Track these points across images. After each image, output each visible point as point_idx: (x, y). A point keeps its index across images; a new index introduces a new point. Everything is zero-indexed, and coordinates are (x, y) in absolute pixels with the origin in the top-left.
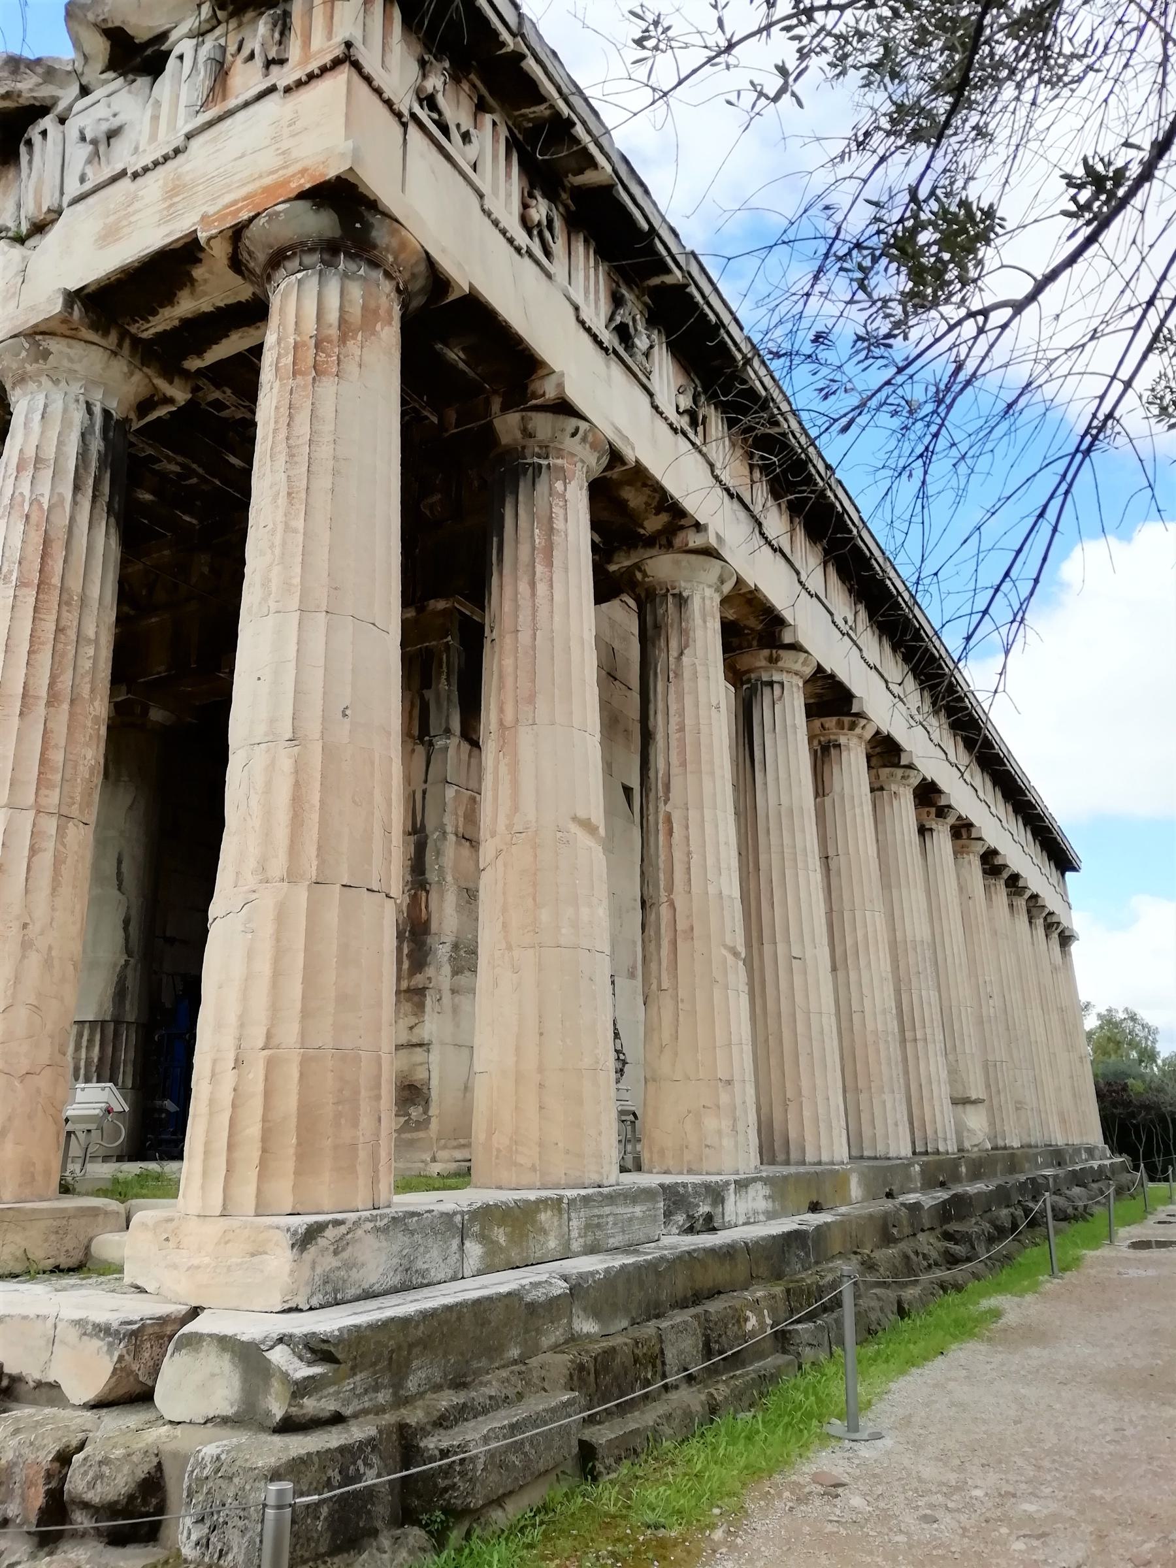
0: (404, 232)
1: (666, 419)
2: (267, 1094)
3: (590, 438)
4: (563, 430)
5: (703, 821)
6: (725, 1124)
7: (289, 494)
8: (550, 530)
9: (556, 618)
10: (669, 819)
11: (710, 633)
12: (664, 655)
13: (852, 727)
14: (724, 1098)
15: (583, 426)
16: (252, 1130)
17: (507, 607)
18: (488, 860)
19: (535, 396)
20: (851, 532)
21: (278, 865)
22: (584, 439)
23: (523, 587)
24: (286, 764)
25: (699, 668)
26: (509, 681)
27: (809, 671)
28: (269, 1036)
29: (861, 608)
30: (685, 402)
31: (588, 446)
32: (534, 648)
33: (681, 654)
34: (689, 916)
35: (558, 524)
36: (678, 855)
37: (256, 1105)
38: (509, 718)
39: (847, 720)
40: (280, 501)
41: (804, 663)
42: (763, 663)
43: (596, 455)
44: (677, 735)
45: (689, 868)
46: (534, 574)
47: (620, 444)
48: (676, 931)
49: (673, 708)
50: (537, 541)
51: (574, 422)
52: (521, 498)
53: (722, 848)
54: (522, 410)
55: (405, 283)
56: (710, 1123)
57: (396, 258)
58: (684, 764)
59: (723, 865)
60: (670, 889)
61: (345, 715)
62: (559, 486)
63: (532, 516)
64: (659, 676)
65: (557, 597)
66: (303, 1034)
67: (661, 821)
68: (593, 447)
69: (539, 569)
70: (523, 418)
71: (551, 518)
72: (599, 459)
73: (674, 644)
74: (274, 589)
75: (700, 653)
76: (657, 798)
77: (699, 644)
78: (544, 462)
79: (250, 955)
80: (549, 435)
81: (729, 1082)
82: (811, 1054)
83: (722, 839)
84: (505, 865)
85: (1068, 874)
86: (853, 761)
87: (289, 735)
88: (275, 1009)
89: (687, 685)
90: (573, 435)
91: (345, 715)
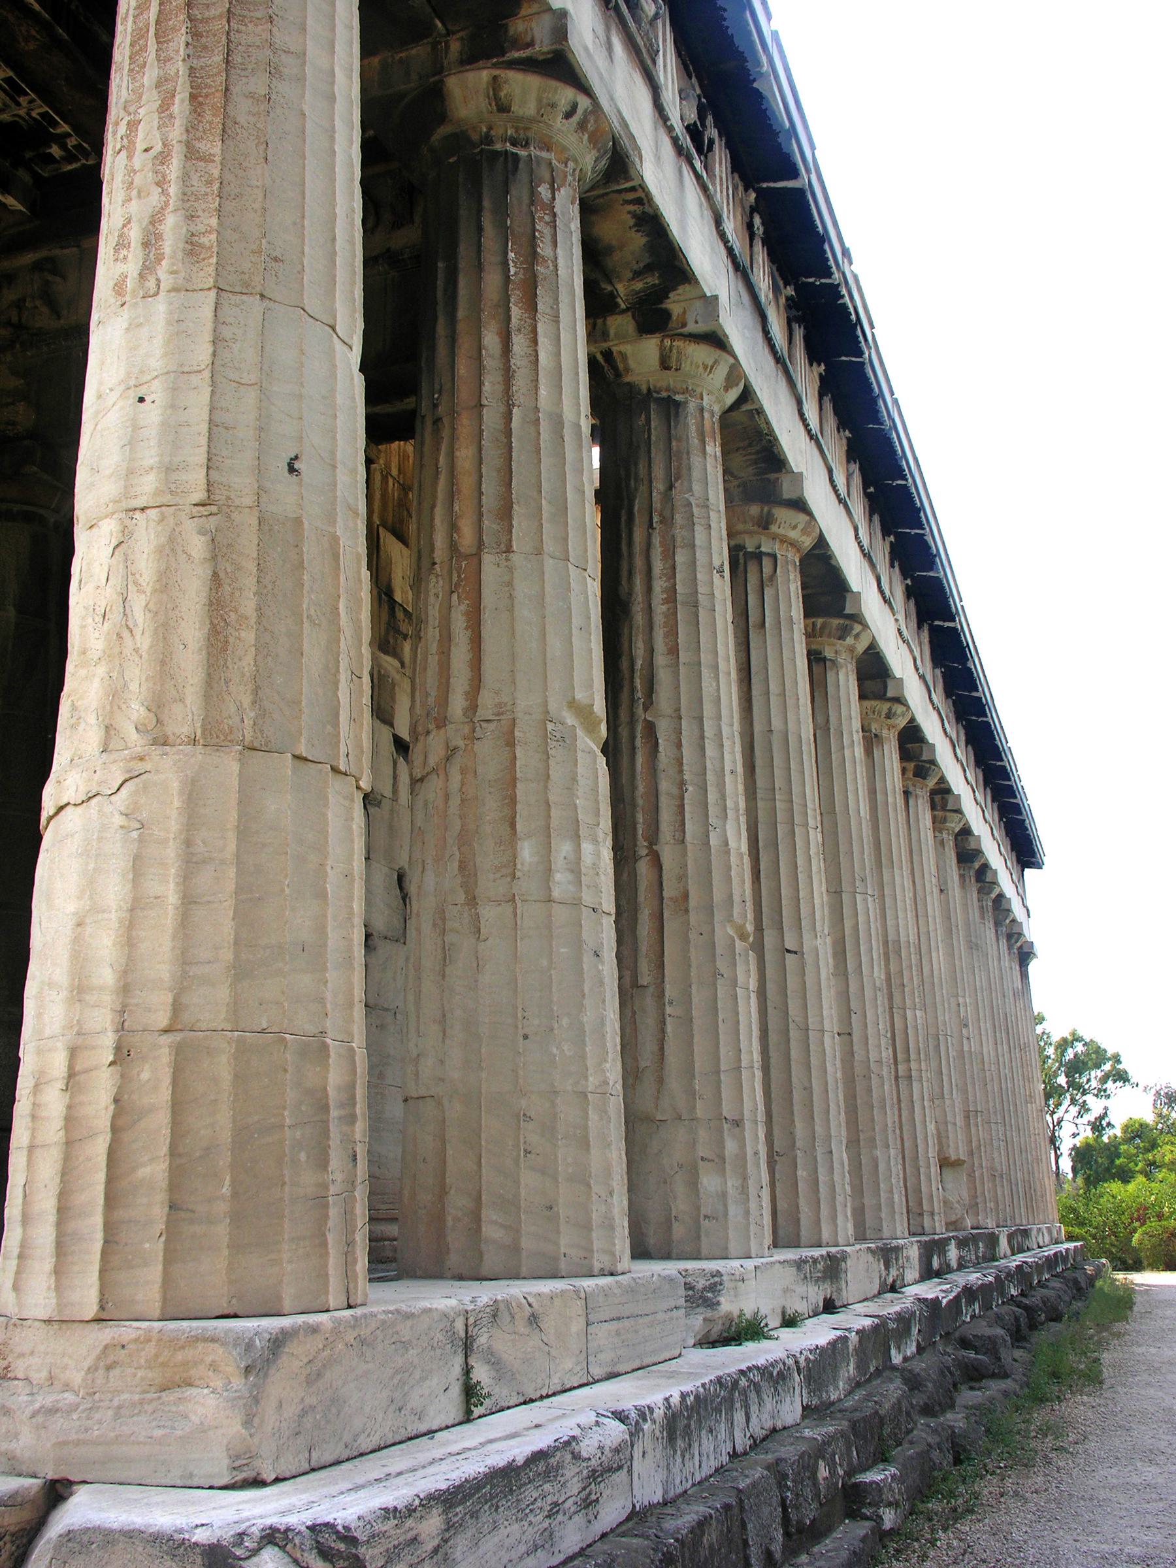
1: (670, 129)
2: (177, 1107)
3: (591, 126)
5: (702, 737)
6: (732, 1183)
7: (193, 97)
8: (533, 256)
9: (543, 392)
10: (651, 728)
11: (710, 462)
12: (643, 488)
13: (843, 633)
14: (731, 1147)
15: (584, 102)
16: (152, 1170)
17: (463, 369)
18: (432, 761)
19: (517, 44)
20: (861, 354)
21: (186, 717)
23: (491, 340)
24: (197, 546)
25: (696, 510)
26: (466, 483)
27: (808, 542)
28: (177, 1008)
29: (855, 467)
30: (692, 116)
32: (508, 433)
33: (671, 487)
34: (682, 877)
35: (544, 249)
36: (665, 786)
37: (158, 1123)
38: (467, 539)
39: (836, 622)
40: (176, 109)
41: (804, 532)
42: (749, 527)
43: (594, 154)
44: (664, 608)
45: (682, 806)
46: (509, 318)
47: (625, 142)
48: (662, 899)
49: (658, 566)
50: (512, 271)
52: (486, 204)
53: (728, 778)
54: (495, 66)
56: (709, 1182)
58: (674, 651)
59: (729, 803)
60: (653, 838)
61: (292, 469)
62: (544, 191)
63: (504, 233)
64: (637, 521)
66: (236, 1006)
67: (639, 735)
68: (594, 139)
69: (516, 312)
70: (495, 78)
73: (658, 472)
74: (167, 249)
75: (697, 487)
76: (633, 701)
77: (696, 474)
78: (523, 153)
79: (138, 868)
81: (738, 1123)
82: (808, 1089)
83: (728, 767)
84: (463, 771)
85: (1027, 871)
86: (846, 682)
87: (199, 495)
88: (184, 959)
89: (679, 533)
90: (568, 115)
91: (292, 469)
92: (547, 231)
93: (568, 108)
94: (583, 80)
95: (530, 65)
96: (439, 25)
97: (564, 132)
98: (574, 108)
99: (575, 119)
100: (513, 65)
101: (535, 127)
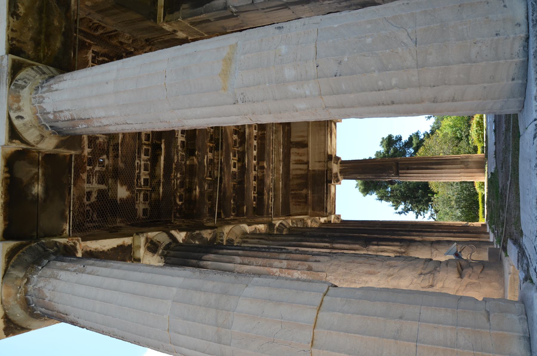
0: (4, 298)
3: (15, 106)
4: (25, 125)
15: (13, 115)
22: (19, 109)
31: (21, 104)
50: (85, 126)
51: (16, 122)
54: (34, 146)
55: (22, 279)
57: (17, 294)
65: (102, 114)
68: (19, 101)
70: (37, 144)
71: (67, 121)
72: (23, 87)
80: (32, 130)
90: (22, 118)
92: (62, 115)
93: (20, 119)
94: (8, 124)
95: (23, 141)
96: (40, 158)
97: (27, 113)
98: (20, 117)
99: (20, 114)
100: (27, 143)
101: (36, 125)
